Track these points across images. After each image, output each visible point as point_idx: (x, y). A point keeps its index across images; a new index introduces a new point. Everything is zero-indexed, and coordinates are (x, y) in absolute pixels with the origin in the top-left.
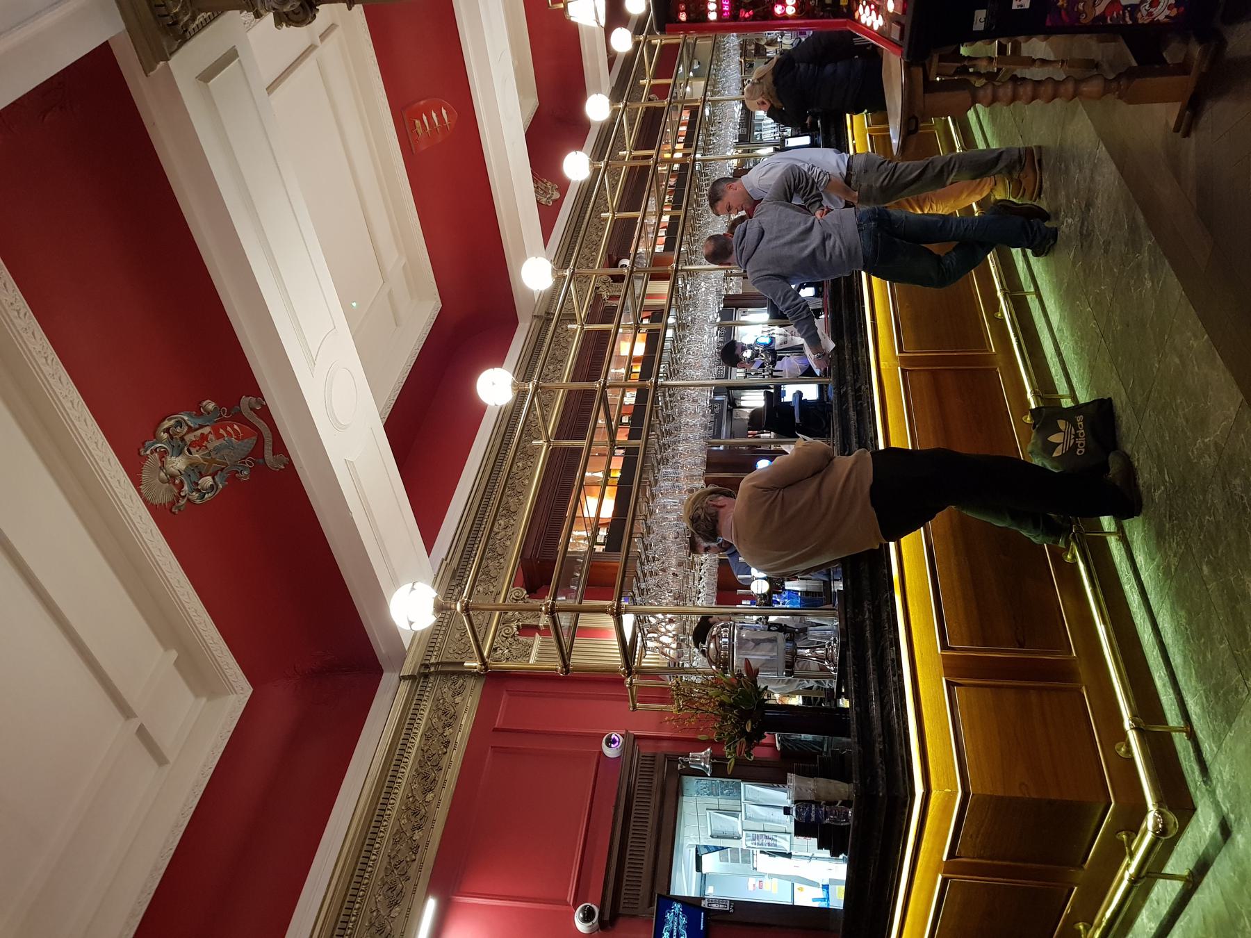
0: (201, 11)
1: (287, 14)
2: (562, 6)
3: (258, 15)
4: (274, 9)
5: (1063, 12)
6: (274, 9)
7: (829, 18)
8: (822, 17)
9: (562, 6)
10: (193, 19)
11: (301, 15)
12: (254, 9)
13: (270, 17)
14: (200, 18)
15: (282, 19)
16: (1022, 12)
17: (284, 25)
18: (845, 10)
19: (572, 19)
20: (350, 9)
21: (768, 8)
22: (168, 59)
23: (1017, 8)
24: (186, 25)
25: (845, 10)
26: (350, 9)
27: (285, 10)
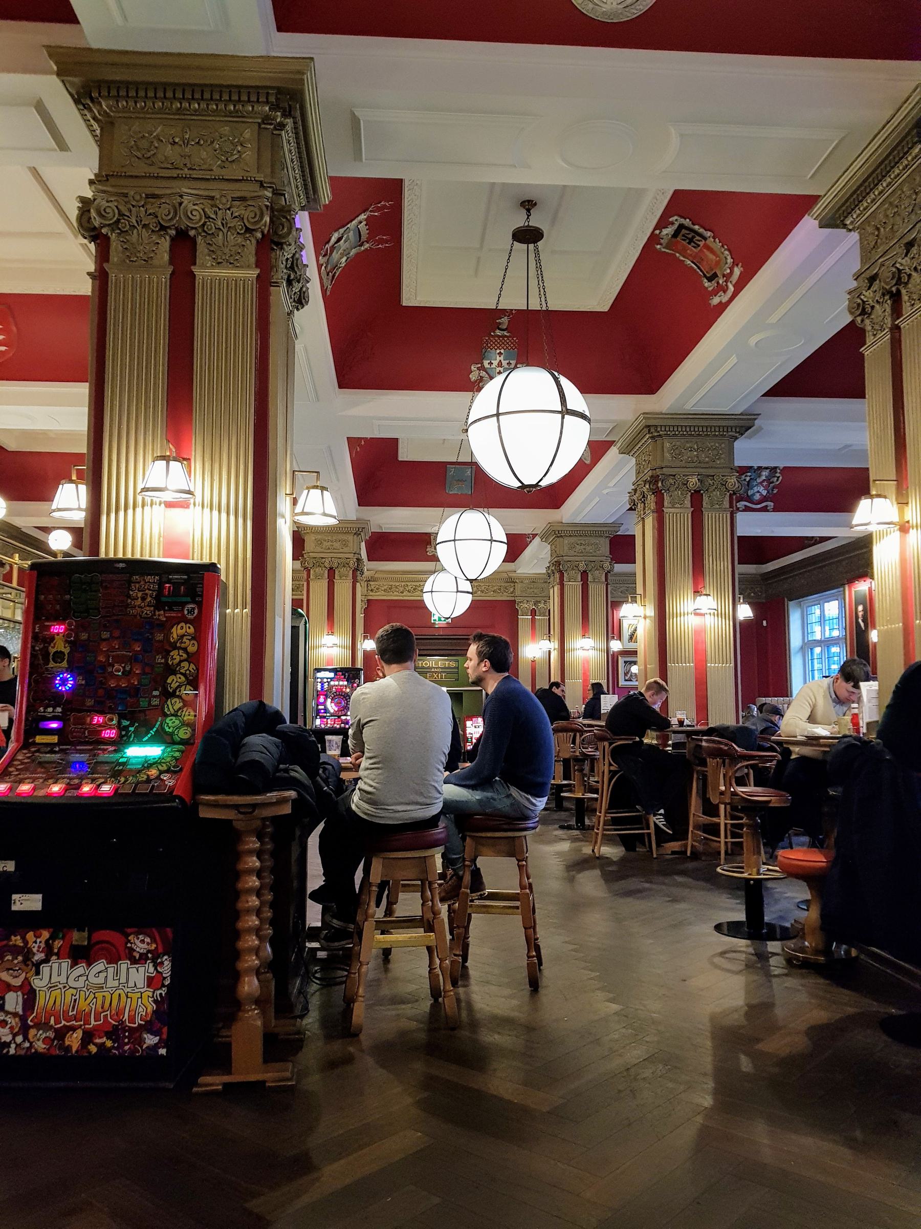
0: (102, 130)
1: (89, 211)
2: (74, 478)
3: (91, 182)
4: (95, 200)
5: (5, 942)
6: (95, 200)
7: (26, 725)
8: (27, 719)
9: (74, 478)
10: (95, 118)
11: (86, 225)
12: (98, 181)
13: (89, 194)
14: (96, 126)
15: (85, 204)
16: (9, 902)
17: (80, 205)
18: (30, 741)
19: (61, 486)
20: (89, 274)
21: (42, 668)
22: (59, 74)
23: (13, 898)
24: (90, 110)
25: (30, 741)
26: (89, 274)
27: (92, 210)
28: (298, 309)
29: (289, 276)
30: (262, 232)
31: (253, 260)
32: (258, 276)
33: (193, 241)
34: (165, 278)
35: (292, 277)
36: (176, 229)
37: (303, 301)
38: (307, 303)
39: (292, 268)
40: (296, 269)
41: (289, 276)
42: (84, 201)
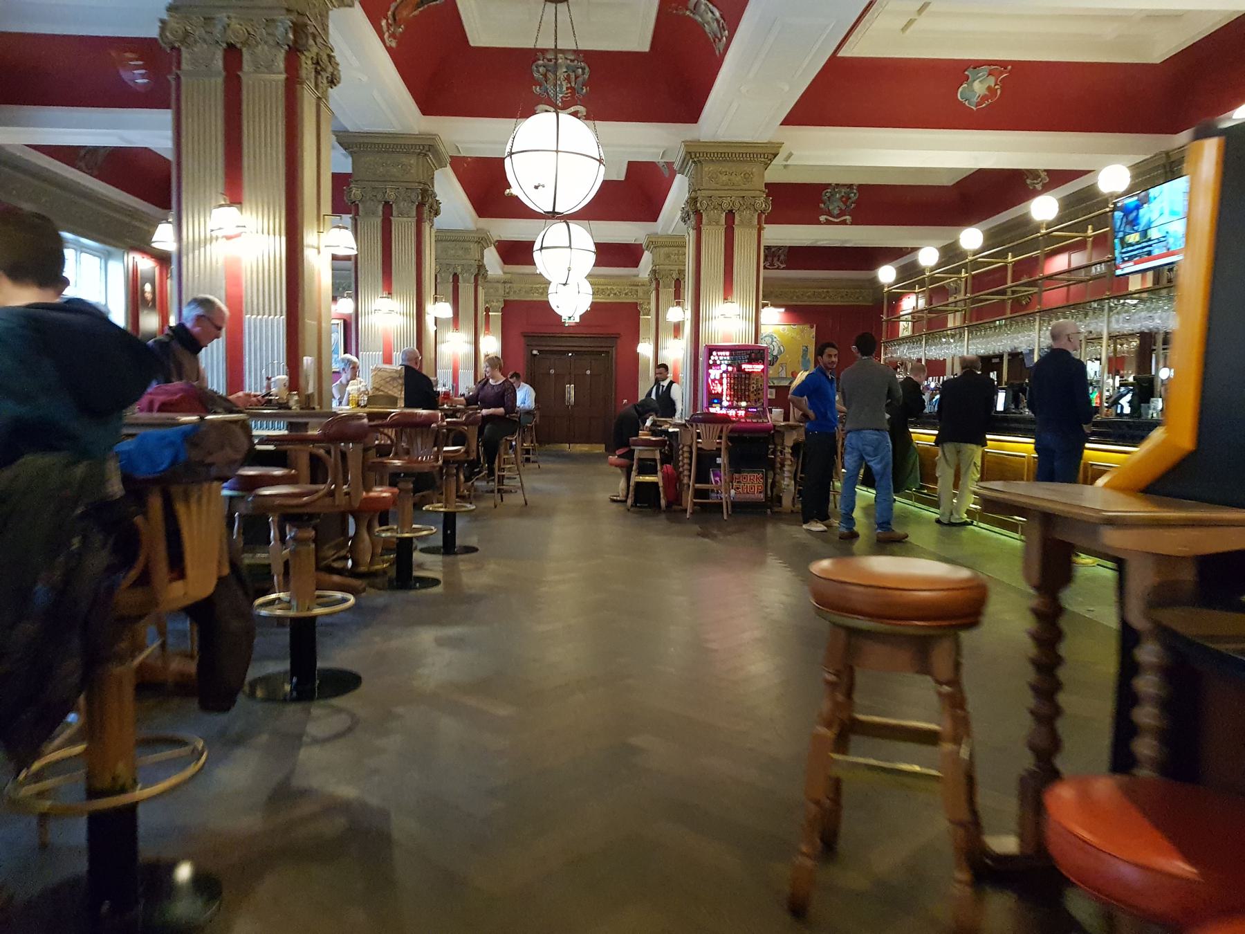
13: (165, 16)
28: (332, 88)
29: (316, 68)
30: (288, 45)
31: (282, 66)
32: (287, 79)
33: (240, 52)
34: (220, 80)
35: (319, 68)
36: (227, 44)
37: (335, 81)
38: (339, 82)
39: (318, 63)
40: (321, 63)
41: (316, 68)
42: (163, 22)
